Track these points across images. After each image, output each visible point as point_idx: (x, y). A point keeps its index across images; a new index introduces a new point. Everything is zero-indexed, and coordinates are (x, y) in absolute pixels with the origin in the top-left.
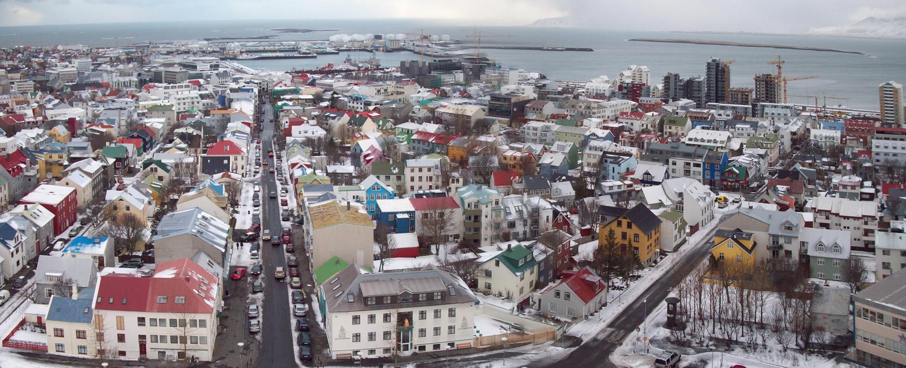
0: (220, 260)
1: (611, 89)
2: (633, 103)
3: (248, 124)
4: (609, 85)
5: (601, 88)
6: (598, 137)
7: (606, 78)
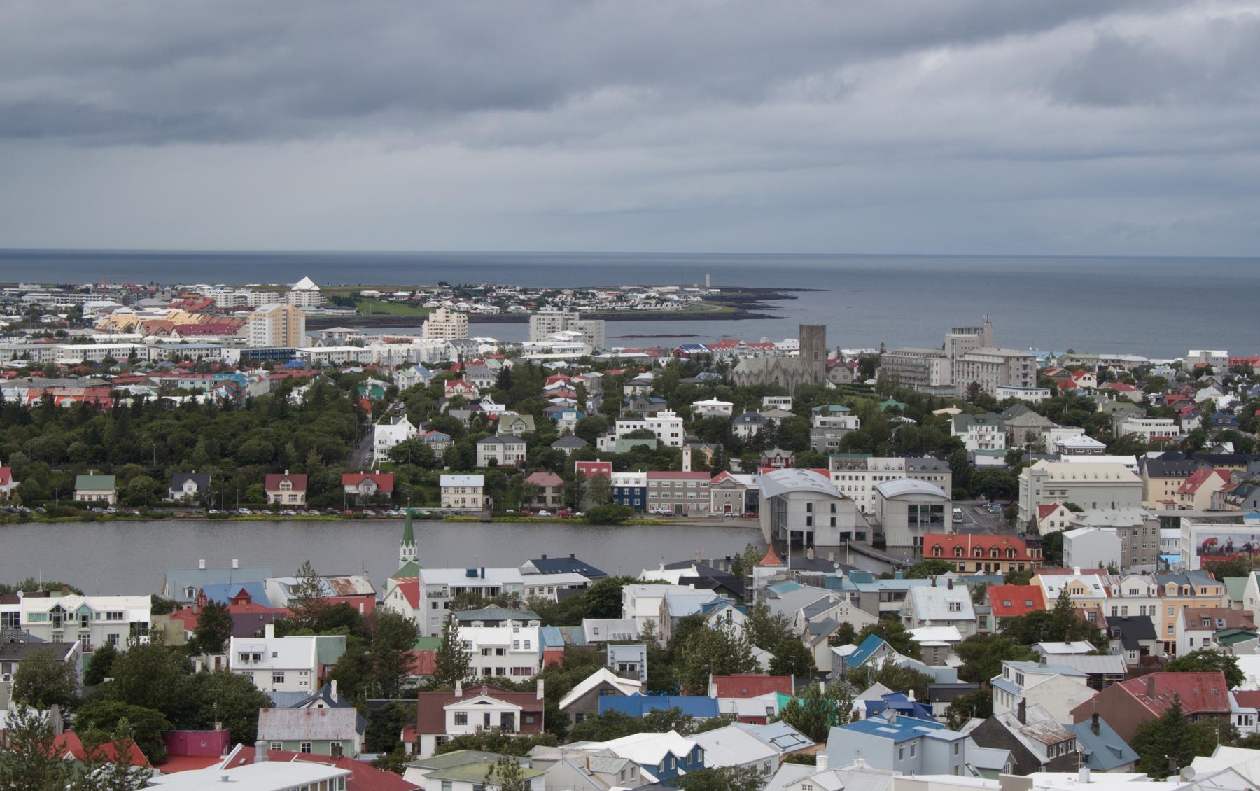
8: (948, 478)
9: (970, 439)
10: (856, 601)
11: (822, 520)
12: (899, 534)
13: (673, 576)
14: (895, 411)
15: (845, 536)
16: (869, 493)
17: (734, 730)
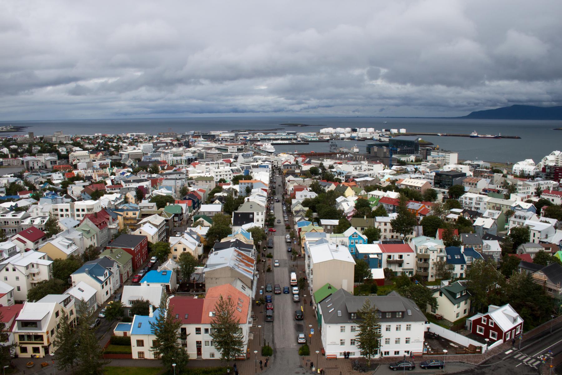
0: (250, 285)
1: (535, 171)
2: (555, 183)
3: (266, 190)
4: (534, 167)
5: (526, 170)
6: (522, 208)
7: (531, 161)
8: (57, 156)
9: (60, 150)
10: (43, 177)
11: (36, 164)
12: (49, 166)
13: (9, 176)
14: (47, 146)
15: (40, 167)
16: (43, 159)
17: (23, 200)
